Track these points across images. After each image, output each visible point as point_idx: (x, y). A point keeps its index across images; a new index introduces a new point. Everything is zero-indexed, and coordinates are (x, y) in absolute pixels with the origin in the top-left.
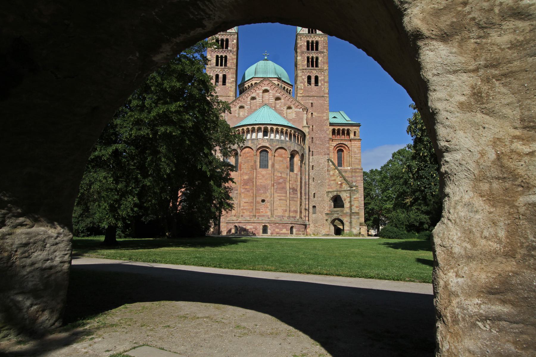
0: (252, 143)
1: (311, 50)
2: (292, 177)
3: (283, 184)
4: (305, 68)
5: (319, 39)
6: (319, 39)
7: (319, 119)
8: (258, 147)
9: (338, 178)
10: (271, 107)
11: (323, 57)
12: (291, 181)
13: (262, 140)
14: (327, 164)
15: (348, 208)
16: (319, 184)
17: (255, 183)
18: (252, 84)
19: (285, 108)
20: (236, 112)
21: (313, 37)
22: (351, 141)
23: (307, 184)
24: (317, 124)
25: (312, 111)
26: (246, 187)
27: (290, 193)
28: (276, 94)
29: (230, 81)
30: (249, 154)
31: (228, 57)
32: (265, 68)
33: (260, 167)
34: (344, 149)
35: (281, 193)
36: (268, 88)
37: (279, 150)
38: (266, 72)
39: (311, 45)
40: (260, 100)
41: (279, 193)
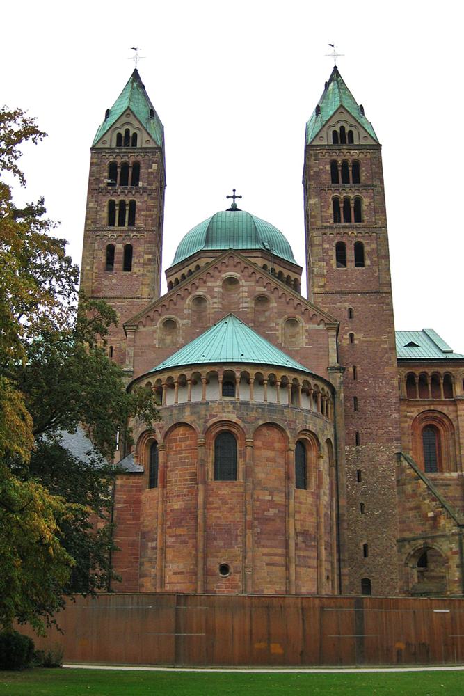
0: (192, 414)
1: (343, 183)
2: (300, 503)
3: (278, 520)
4: (328, 224)
5: (361, 156)
6: (361, 156)
7: (371, 350)
8: (208, 425)
9: (427, 501)
10: (244, 320)
11: (373, 198)
12: (299, 512)
13: (220, 407)
14: (396, 465)
15: (455, 582)
16: (376, 519)
17: (200, 520)
18: (198, 267)
19: (281, 321)
20: (156, 336)
21: (345, 151)
22: (456, 405)
23: (343, 521)
24: (366, 361)
25: (352, 330)
26: (179, 531)
27: (296, 544)
28: (258, 289)
29: (141, 261)
30: (187, 443)
31: (138, 204)
32: (232, 227)
33: (216, 479)
34: (439, 426)
35: (273, 547)
36: (237, 275)
37: (265, 431)
38: (233, 238)
39: (342, 171)
40: (215, 306)
41: (267, 547)
